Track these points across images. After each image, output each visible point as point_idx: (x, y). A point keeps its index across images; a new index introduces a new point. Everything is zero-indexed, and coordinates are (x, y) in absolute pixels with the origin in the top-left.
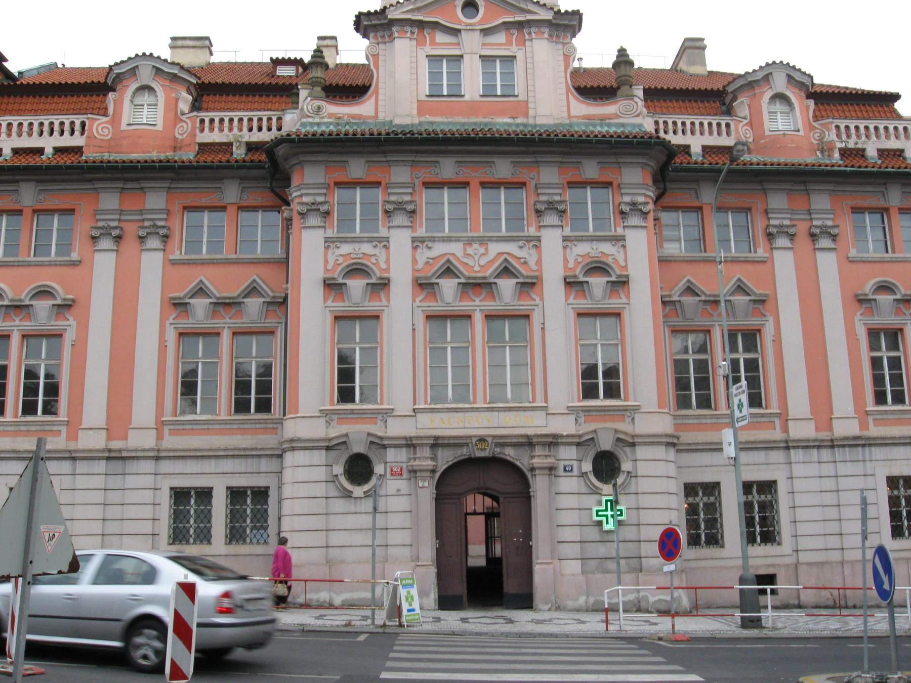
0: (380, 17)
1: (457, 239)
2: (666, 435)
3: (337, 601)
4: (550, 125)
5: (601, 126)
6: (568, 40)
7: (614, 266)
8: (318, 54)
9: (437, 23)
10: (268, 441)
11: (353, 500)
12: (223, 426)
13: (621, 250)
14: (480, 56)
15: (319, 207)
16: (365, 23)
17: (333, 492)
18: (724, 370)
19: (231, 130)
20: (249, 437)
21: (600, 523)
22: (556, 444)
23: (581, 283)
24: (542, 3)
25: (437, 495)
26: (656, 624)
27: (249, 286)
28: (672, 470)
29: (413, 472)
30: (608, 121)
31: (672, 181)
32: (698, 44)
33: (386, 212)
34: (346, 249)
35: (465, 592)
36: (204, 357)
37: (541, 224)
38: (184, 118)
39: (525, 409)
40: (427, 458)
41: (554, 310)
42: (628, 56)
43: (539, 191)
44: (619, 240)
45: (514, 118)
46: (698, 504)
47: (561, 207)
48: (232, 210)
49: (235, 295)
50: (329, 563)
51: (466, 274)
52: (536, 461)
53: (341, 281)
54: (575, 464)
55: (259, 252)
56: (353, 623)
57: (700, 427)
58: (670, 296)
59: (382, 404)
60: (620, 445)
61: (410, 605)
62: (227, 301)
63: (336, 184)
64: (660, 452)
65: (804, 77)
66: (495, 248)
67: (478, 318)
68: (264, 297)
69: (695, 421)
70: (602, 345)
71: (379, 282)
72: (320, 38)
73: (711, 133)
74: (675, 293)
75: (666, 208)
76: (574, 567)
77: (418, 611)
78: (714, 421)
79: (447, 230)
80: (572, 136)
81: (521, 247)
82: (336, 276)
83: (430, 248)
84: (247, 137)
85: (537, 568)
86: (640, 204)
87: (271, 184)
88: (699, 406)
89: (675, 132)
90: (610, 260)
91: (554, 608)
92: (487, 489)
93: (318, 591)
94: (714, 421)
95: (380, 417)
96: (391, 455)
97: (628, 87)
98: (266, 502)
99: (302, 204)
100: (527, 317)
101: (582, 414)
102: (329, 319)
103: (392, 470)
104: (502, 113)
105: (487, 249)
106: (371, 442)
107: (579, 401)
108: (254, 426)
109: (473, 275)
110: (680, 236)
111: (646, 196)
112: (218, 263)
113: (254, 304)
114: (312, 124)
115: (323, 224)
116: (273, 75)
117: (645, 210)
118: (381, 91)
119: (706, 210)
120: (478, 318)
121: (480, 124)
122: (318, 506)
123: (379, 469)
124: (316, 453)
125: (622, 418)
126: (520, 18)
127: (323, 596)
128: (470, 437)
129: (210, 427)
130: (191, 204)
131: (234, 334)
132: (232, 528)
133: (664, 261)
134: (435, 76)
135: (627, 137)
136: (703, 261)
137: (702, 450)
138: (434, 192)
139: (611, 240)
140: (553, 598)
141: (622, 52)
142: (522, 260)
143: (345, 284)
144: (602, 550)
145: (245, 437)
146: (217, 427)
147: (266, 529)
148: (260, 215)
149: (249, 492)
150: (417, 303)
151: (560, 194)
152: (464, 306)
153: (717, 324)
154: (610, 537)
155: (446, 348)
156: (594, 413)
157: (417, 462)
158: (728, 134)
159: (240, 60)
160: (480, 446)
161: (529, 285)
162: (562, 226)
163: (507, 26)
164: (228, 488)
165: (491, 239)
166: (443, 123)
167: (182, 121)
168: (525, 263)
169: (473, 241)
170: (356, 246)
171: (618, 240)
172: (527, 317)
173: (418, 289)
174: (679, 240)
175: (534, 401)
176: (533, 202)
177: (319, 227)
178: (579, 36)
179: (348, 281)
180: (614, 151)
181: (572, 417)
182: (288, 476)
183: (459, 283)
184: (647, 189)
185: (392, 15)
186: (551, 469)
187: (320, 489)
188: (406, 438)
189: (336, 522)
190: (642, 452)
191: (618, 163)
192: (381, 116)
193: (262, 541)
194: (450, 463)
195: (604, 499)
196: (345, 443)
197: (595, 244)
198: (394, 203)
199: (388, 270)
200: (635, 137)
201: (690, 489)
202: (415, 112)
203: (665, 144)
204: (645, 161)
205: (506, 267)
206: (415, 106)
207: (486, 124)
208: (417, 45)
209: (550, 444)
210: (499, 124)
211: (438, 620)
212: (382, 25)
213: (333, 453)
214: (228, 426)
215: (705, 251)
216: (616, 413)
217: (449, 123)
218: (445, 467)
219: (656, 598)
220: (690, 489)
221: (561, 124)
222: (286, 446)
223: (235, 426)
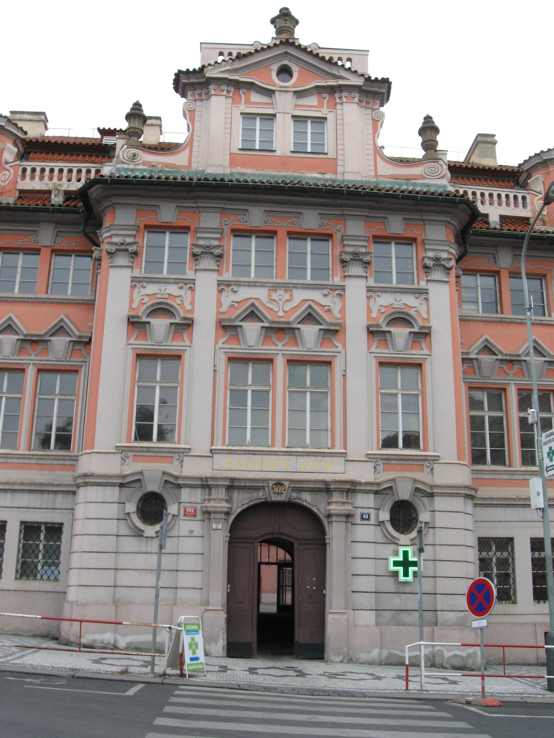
0: (198, 75)
1: (262, 285)
2: (465, 487)
3: (122, 642)
4: (358, 181)
5: (407, 185)
6: (377, 106)
7: (417, 318)
8: (137, 107)
9: (252, 84)
10: (64, 477)
11: (144, 540)
12: (21, 461)
13: (424, 303)
14: (293, 116)
15: (128, 247)
16: (184, 81)
17: (124, 530)
18: (533, 417)
19: (51, 179)
20: (47, 472)
21: (396, 574)
22: (354, 491)
23: (384, 332)
24: (353, 70)
25: (230, 538)
26: (455, 683)
27: (56, 325)
28: (469, 522)
29: (207, 513)
30: (413, 181)
32: (489, 139)
33: (194, 255)
34: (152, 289)
35: (255, 639)
36: (8, 391)
37: (346, 274)
38: (7, 166)
39: (323, 454)
40: (222, 500)
41: (356, 358)
42: (433, 122)
43: (346, 242)
44: (422, 293)
45: (323, 174)
46: (491, 559)
47: (366, 259)
48: (45, 253)
49: (42, 332)
50: (116, 603)
51: (270, 318)
52: (332, 507)
53: (144, 319)
54: (372, 512)
55: (69, 294)
56: (131, 669)
57: (495, 483)
58: (468, 353)
59: (179, 443)
60: (419, 494)
61: (194, 653)
62: (35, 338)
63: (146, 227)
64: (458, 504)
66: (299, 295)
67: (280, 363)
68: (70, 336)
69: (490, 477)
70: (402, 395)
71: (182, 322)
73: (508, 204)
74: (473, 351)
76: (368, 618)
77: (202, 659)
78: (508, 477)
79: (253, 275)
81: (325, 295)
82: (140, 314)
83: (235, 292)
84: (66, 186)
85: (330, 618)
86: (444, 259)
87: (84, 228)
88: (494, 462)
90: (412, 312)
91: (346, 660)
92: (282, 534)
93: (103, 632)
94: (508, 477)
95: (176, 456)
96: (185, 495)
97: (433, 151)
98: (59, 539)
99: (112, 243)
100: (329, 363)
101: (380, 462)
102: (131, 356)
103: (185, 511)
104: (311, 168)
105: (291, 296)
106: (166, 482)
107: (379, 449)
108: (52, 462)
109: (276, 319)
110: (477, 297)
111: (449, 253)
112: (28, 302)
113: (60, 343)
115: (130, 264)
119: (504, 275)
120: (280, 363)
121: (290, 177)
122: (109, 543)
123: (172, 509)
124: (109, 489)
125: (421, 468)
126: (332, 83)
127: (108, 637)
128: (267, 480)
129: (9, 461)
130: (6, 246)
131: (39, 370)
132: (24, 563)
133: (463, 320)
134: (248, 131)
135: (433, 194)
136: (500, 322)
137: (497, 505)
138: (242, 242)
139: (415, 293)
140: (345, 649)
141: (428, 119)
142: (326, 308)
143: (149, 323)
144: (397, 602)
145: (43, 472)
146: (16, 461)
147: (57, 566)
148: (73, 259)
149: (43, 528)
150: (220, 345)
151: (366, 247)
152: (267, 349)
153: (512, 382)
154: (407, 589)
155: (246, 391)
156: (393, 462)
157: (212, 504)
158: (524, 206)
160: (276, 490)
161: (333, 332)
162: (366, 277)
163: (319, 89)
164: (22, 523)
165: (296, 286)
166: (254, 175)
167: (6, 169)
168: (329, 311)
169: (278, 287)
170: (162, 287)
171: (422, 294)
172: (329, 363)
173: (221, 331)
174: (477, 302)
175: (333, 446)
176: (339, 253)
177: (127, 267)
178: (386, 106)
179: (152, 320)
180: (419, 207)
181: (371, 465)
182: (80, 511)
183: (262, 327)
184: (451, 247)
185: (209, 74)
186: (348, 516)
187: (112, 527)
188: (201, 479)
189: (126, 561)
190: (440, 503)
191: (422, 220)
192: (194, 166)
193: (52, 578)
194: (245, 506)
195: (401, 549)
196: (139, 481)
197: (398, 296)
198: (202, 246)
199: (192, 311)
200: (440, 194)
201: (484, 543)
202: (227, 163)
204: (448, 219)
205: (309, 314)
206: (228, 157)
207: (295, 178)
208: (233, 103)
209: (348, 491)
210: (307, 178)
211: (224, 669)
212: (200, 84)
213: (127, 491)
214: (26, 461)
215: (502, 313)
216: (415, 463)
217: (260, 175)
218: (239, 510)
219: (452, 653)
220: (484, 543)
221: (368, 182)
222: (79, 481)
223: (34, 461)
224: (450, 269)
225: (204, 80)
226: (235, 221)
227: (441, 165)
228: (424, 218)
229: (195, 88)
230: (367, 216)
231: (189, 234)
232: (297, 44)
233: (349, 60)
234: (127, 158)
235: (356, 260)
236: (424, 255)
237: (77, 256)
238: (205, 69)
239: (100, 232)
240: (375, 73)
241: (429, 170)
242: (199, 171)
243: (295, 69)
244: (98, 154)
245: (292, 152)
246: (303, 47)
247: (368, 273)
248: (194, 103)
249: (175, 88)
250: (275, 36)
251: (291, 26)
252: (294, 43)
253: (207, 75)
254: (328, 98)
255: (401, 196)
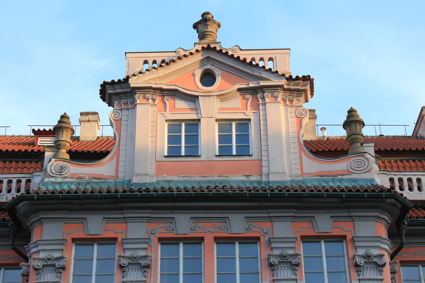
5: (333, 181)
9: (176, 90)
14: (217, 120)
16: (110, 92)
31: (409, 235)
42: (358, 116)
43: (273, 245)
72: (82, 114)
75: (404, 263)
80: (304, 191)
87: (13, 242)
89: (411, 189)
114: (53, 183)
116: (33, 144)
117: (380, 263)
118: (121, 153)
141: (351, 112)
159: (10, 133)
185: (134, 82)
192: (121, 175)
198: (129, 258)
202: (153, 172)
203: (399, 199)
207: (221, 182)
210: (233, 181)
217: (186, 181)
224: (384, 266)
225: (129, 90)
226: (162, 230)
227: (366, 159)
228: (352, 214)
229: (120, 97)
230: (294, 217)
231: (117, 245)
232: (218, 49)
233: (271, 59)
234: (54, 172)
235: (284, 262)
236: (355, 253)
237: (6, 269)
238: (130, 79)
239: (28, 247)
240: (296, 72)
241: (356, 165)
242: (126, 180)
243: (217, 72)
244: (30, 160)
245: (217, 156)
246: (224, 52)
247: (298, 276)
248: (120, 112)
249: (101, 97)
250: (197, 40)
251: (213, 31)
252: (215, 48)
253: (131, 86)
254: (251, 100)
255: (325, 195)
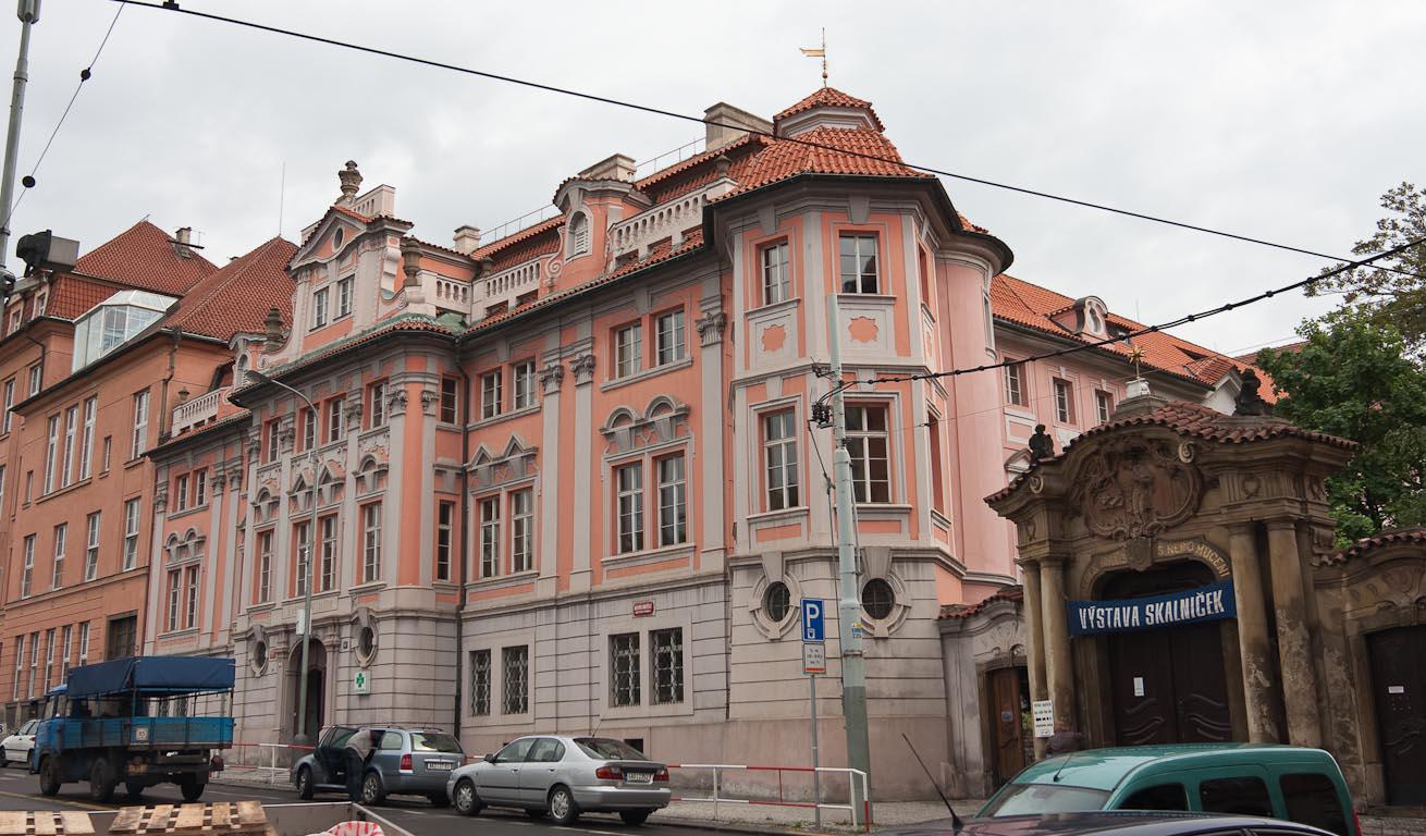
65: (596, 184)
74: (473, 463)
111: (406, 383)
243: (344, 230)
